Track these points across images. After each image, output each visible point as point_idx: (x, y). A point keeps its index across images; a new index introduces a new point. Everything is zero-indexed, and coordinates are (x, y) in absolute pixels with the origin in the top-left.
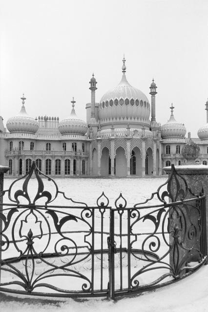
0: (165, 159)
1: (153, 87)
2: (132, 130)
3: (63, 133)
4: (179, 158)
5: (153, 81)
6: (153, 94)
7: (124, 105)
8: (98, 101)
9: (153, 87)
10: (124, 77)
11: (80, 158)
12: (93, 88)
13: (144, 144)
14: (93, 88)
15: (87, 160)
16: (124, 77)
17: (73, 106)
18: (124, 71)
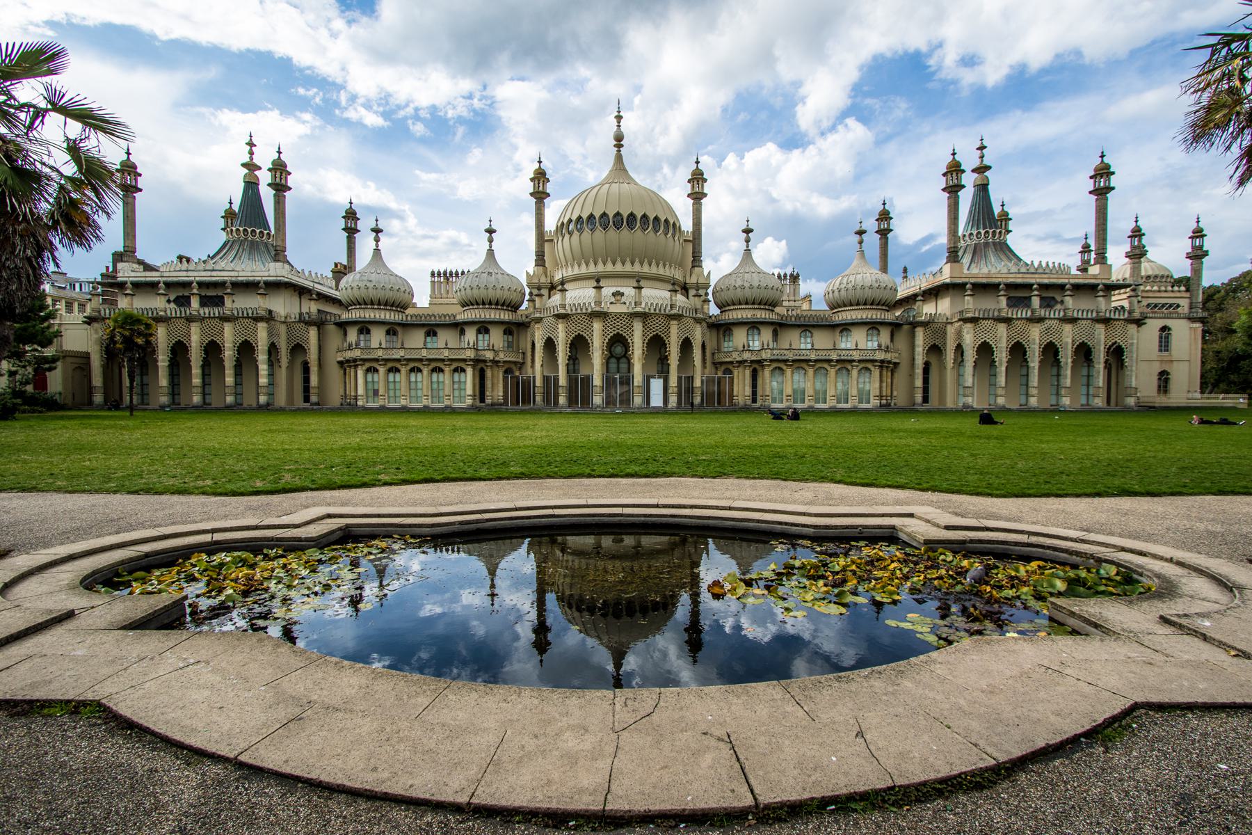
0: (722, 363)
1: (698, 178)
2: (607, 291)
3: (465, 304)
4: (752, 362)
5: (697, 162)
6: (697, 197)
7: (599, 232)
8: (550, 224)
9: (698, 178)
10: (619, 158)
11: (495, 362)
12: (540, 196)
13: (638, 327)
14: (540, 196)
15: (520, 369)
16: (619, 158)
17: (491, 241)
18: (619, 138)
